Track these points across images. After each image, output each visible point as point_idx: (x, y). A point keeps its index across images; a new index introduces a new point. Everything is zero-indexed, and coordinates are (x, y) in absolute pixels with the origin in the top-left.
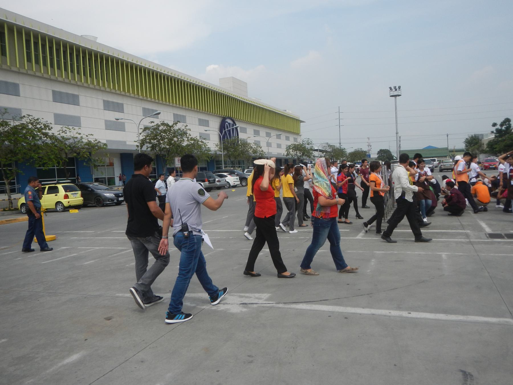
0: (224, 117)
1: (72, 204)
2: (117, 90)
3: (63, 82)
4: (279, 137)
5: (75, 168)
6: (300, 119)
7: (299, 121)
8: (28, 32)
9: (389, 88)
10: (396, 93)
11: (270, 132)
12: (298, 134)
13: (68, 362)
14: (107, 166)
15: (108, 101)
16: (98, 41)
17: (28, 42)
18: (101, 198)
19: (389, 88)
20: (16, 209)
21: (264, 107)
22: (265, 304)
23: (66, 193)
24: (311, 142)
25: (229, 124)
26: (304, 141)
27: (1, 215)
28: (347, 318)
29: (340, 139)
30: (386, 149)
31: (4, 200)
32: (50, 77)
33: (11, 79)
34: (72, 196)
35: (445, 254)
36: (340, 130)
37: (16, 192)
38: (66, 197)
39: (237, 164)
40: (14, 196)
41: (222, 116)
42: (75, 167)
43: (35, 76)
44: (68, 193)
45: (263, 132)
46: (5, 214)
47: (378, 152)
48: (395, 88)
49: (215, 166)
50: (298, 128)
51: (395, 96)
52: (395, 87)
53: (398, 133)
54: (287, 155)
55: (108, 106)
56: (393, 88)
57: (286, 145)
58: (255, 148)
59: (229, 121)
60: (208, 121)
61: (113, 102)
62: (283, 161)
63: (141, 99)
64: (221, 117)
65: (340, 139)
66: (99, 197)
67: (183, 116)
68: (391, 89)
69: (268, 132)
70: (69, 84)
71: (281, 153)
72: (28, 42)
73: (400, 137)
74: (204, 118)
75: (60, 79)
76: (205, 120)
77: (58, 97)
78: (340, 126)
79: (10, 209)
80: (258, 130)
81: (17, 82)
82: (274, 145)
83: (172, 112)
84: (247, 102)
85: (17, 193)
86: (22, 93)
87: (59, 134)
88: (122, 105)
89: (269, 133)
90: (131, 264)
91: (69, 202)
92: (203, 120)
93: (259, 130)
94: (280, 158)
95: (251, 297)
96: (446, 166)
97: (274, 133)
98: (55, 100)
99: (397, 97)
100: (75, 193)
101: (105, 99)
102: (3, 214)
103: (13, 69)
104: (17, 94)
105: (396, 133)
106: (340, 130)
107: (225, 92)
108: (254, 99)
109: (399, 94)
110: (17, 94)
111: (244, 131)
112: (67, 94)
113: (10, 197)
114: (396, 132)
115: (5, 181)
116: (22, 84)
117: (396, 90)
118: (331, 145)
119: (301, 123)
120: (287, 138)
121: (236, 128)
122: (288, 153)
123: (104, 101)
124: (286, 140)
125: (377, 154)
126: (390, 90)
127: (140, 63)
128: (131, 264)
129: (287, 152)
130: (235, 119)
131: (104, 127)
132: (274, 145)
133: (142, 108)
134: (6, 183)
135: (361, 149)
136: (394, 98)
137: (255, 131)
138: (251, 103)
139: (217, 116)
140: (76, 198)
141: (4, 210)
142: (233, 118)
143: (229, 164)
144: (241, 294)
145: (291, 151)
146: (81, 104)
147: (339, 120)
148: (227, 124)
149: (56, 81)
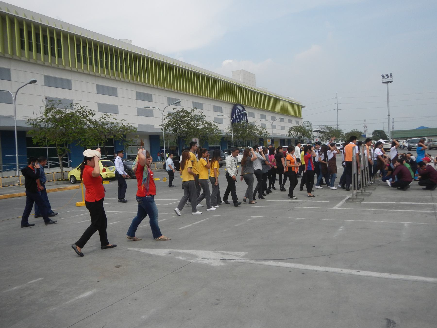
1: (109, 176)
2: (147, 83)
3: (105, 78)
4: (282, 120)
5: (113, 147)
6: (302, 105)
7: (300, 107)
8: (78, 38)
9: (382, 75)
10: (388, 80)
12: (300, 118)
13: (83, 297)
14: (139, 145)
15: (140, 93)
16: (132, 44)
17: (78, 46)
18: (131, 172)
19: (382, 75)
20: (67, 180)
21: (270, 95)
22: (241, 260)
23: (104, 167)
24: (310, 125)
25: (239, 110)
26: (304, 123)
27: (55, 184)
28: (304, 274)
29: (338, 121)
30: (380, 130)
31: (58, 172)
32: (95, 74)
34: (109, 169)
35: (408, 223)
36: (337, 113)
37: (68, 166)
38: (104, 170)
40: (65, 169)
41: (234, 103)
42: (113, 146)
43: (83, 73)
44: (106, 168)
45: (269, 116)
46: (58, 184)
47: (373, 132)
48: (387, 75)
49: (228, 145)
50: (300, 113)
52: (387, 75)
53: (390, 116)
54: (290, 136)
55: (140, 96)
56: (385, 75)
57: (289, 127)
58: (260, 130)
59: (240, 107)
60: (221, 108)
61: (144, 93)
62: (286, 141)
63: (167, 91)
65: (338, 121)
66: (130, 171)
67: (201, 103)
68: (383, 76)
69: (273, 116)
70: (110, 79)
71: (285, 134)
72: (78, 46)
73: (393, 119)
74: (218, 105)
75: (102, 75)
76: (219, 107)
77: (101, 90)
78: (337, 110)
79: (63, 180)
80: (265, 114)
82: (278, 127)
83: (192, 101)
84: (255, 90)
85: (69, 167)
86: (73, 88)
87: (100, 120)
88: (151, 95)
89: (274, 117)
90: (144, 226)
91: (106, 175)
92: (217, 107)
94: (283, 139)
95: (230, 254)
96: (435, 144)
97: (278, 117)
98: (98, 93)
99: (389, 84)
100: (111, 168)
101: (138, 91)
102: (57, 183)
103: (67, 68)
104: (70, 88)
105: (388, 116)
106: (337, 113)
107: (236, 83)
108: (261, 88)
109: (391, 80)
110: (70, 88)
111: (252, 115)
112: (108, 87)
113: (62, 170)
114: (388, 115)
115: (59, 157)
116: (74, 80)
117: (388, 77)
118: (329, 126)
119: (302, 108)
120: (290, 121)
121: (246, 114)
122: (289, 134)
123: (137, 92)
124: (289, 123)
125: (372, 134)
126: (382, 77)
127: (166, 60)
128: (144, 226)
129: (289, 133)
130: (244, 106)
131: (136, 114)
132: (278, 127)
134: (60, 159)
135: (357, 130)
136: (386, 84)
137: (261, 115)
138: (259, 92)
139: (229, 103)
140: (112, 171)
141: (58, 181)
142: (243, 105)
143: (239, 144)
144: (225, 252)
145: (292, 132)
146: (118, 95)
147: (337, 105)
149: (99, 77)
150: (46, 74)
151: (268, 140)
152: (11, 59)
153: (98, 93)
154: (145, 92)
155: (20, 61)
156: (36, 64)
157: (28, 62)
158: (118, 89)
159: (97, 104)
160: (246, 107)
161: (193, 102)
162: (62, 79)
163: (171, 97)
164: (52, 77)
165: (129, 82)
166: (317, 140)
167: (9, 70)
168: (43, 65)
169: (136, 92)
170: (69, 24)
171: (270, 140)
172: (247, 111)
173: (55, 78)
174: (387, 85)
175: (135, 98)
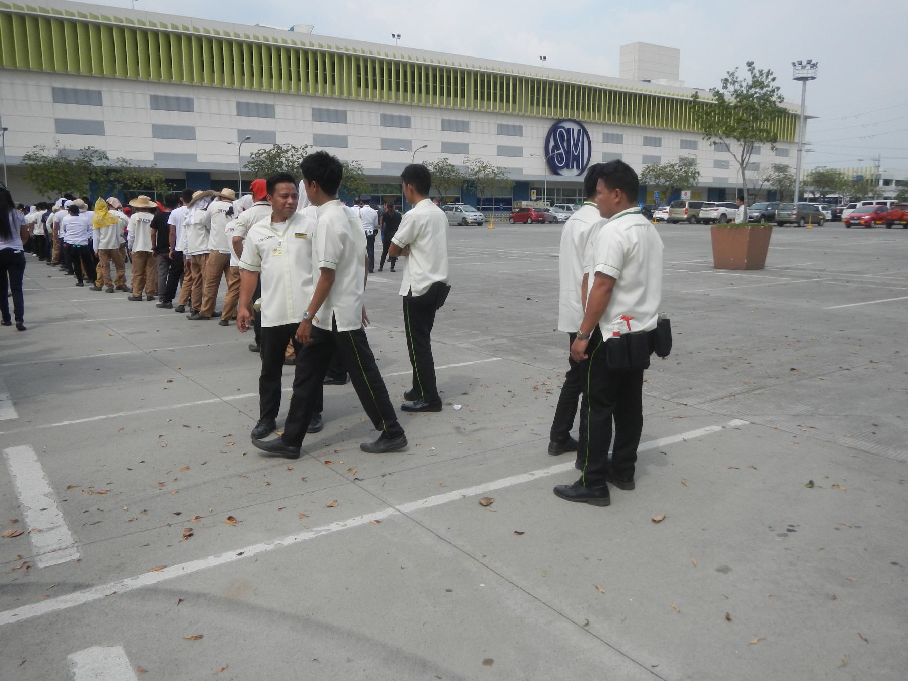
0: (561, 119)
3: (251, 91)
11: (696, 140)
15: (320, 110)
25: (568, 131)
33: (183, 94)
39: (580, 195)
41: (555, 117)
51: (804, 79)
59: (567, 125)
60: (520, 127)
61: (328, 111)
64: (553, 119)
67: (463, 122)
69: (688, 139)
70: (260, 92)
76: (514, 126)
77: (243, 110)
80: (658, 136)
81: (191, 96)
88: (345, 113)
89: (690, 141)
92: (508, 126)
93: (661, 137)
98: (239, 113)
101: (316, 106)
116: (198, 98)
119: (808, 120)
123: (313, 109)
133: (379, 116)
136: (801, 82)
139: (541, 118)
142: (583, 120)
148: (561, 133)
149: (240, 90)
150: (152, 93)
151: (532, 191)
152: (102, 78)
153: (239, 113)
154: (332, 108)
155: (113, 79)
156: (136, 81)
157: (125, 80)
158: (275, 106)
159: (236, 131)
160: (596, 123)
161: (443, 121)
162: (178, 99)
163: (388, 113)
164: (161, 97)
165: (296, 94)
166: (686, 195)
167: (99, 93)
168: (148, 82)
169: (311, 109)
170: (191, 18)
171: (535, 191)
172: (596, 134)
173: (167, 98)
174: (804, 85)
175: (311, 118)
